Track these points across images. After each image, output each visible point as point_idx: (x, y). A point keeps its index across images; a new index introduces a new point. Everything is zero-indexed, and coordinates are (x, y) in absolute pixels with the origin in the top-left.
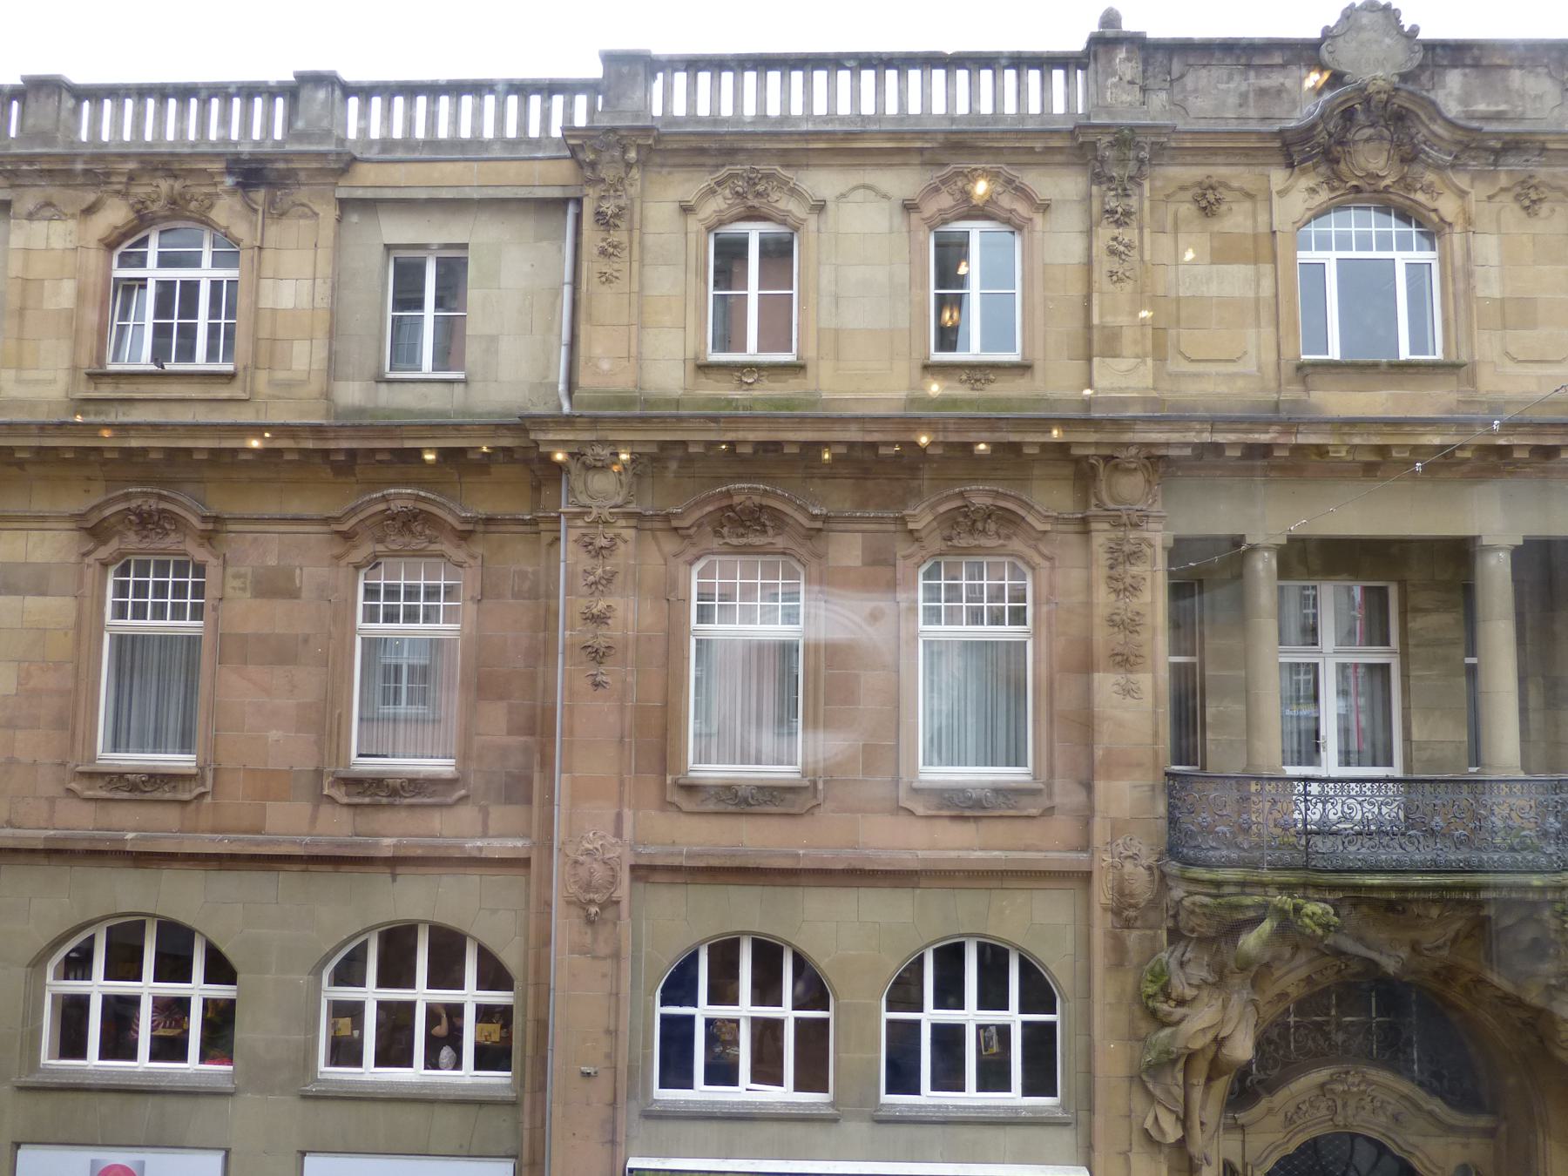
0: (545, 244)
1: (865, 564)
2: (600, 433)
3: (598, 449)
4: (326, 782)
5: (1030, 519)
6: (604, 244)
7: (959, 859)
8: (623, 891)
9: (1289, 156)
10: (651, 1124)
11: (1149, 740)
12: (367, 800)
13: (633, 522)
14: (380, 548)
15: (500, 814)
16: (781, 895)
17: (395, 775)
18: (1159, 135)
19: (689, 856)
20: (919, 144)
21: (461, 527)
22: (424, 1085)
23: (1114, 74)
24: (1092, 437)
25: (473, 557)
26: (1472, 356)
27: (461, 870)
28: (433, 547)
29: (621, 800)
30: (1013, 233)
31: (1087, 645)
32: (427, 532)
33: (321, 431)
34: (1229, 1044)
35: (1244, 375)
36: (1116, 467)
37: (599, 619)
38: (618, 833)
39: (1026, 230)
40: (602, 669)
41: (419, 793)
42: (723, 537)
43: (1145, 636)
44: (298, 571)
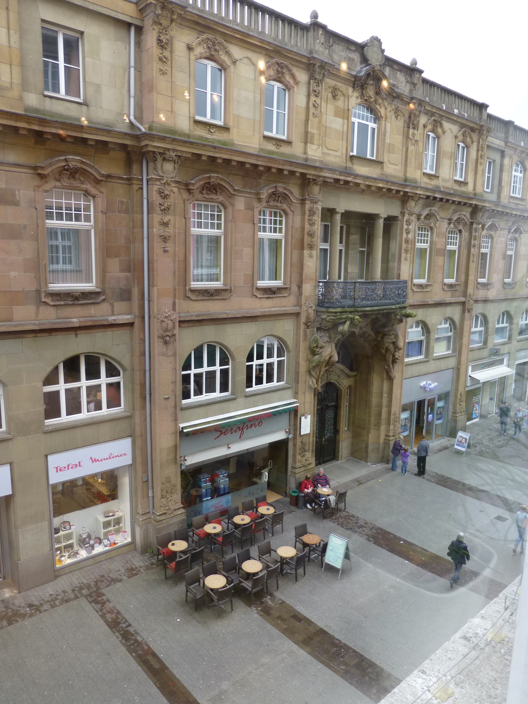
0: (119, 43)
1: (245, 209)
2: (174, 146)
3: (171, 153)
4: (43, 295)
5: (291, 198)
6: (161, 56)
7: (270, 311)
8: (176, 331)
9: (354, 84)
10: (184, 412)
11: (314, 271)
12: (62, 303)
13: (177, 185)
14: (58, 184)
15: (119, 306)
16: (221, 327)
17: (75, 291)
18: (330, 67)
19: (197, 316)
20: (267, 47)
21: (100, 178)
22: (108, 415)
23: (318, 39)
24: (313, 172)
25: (102, 193)
26: (383, 160)
27: (105, 330)
28: (83, 186)
29: (175, 297)
30: (220, 70)
31: (302, 241)
32: (82, 179)
33: (43, 122)
34: (333, 357)
35: (339, 157)
36: (315, 183)
37: (165, 224)
38: (174, 309)
39: (291, 91)
40: (167, 245)
41: (85, 299)
42: (203, 194)
43: (315, 239)
44: (17, 192)
